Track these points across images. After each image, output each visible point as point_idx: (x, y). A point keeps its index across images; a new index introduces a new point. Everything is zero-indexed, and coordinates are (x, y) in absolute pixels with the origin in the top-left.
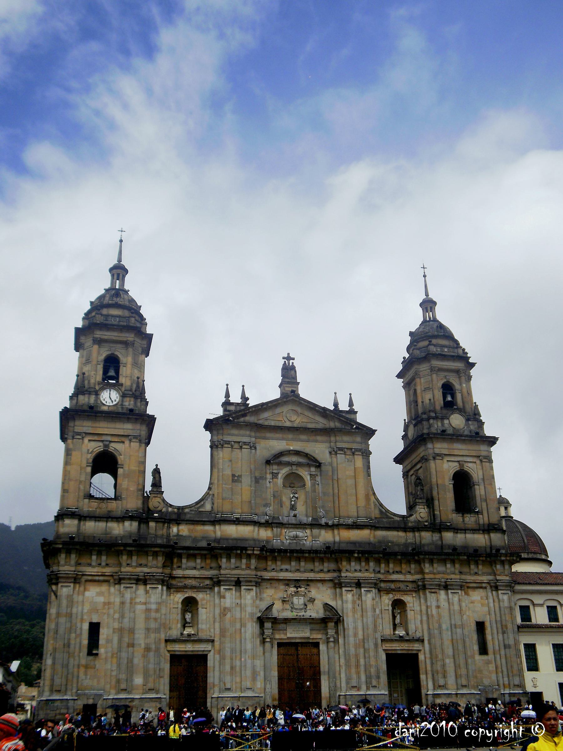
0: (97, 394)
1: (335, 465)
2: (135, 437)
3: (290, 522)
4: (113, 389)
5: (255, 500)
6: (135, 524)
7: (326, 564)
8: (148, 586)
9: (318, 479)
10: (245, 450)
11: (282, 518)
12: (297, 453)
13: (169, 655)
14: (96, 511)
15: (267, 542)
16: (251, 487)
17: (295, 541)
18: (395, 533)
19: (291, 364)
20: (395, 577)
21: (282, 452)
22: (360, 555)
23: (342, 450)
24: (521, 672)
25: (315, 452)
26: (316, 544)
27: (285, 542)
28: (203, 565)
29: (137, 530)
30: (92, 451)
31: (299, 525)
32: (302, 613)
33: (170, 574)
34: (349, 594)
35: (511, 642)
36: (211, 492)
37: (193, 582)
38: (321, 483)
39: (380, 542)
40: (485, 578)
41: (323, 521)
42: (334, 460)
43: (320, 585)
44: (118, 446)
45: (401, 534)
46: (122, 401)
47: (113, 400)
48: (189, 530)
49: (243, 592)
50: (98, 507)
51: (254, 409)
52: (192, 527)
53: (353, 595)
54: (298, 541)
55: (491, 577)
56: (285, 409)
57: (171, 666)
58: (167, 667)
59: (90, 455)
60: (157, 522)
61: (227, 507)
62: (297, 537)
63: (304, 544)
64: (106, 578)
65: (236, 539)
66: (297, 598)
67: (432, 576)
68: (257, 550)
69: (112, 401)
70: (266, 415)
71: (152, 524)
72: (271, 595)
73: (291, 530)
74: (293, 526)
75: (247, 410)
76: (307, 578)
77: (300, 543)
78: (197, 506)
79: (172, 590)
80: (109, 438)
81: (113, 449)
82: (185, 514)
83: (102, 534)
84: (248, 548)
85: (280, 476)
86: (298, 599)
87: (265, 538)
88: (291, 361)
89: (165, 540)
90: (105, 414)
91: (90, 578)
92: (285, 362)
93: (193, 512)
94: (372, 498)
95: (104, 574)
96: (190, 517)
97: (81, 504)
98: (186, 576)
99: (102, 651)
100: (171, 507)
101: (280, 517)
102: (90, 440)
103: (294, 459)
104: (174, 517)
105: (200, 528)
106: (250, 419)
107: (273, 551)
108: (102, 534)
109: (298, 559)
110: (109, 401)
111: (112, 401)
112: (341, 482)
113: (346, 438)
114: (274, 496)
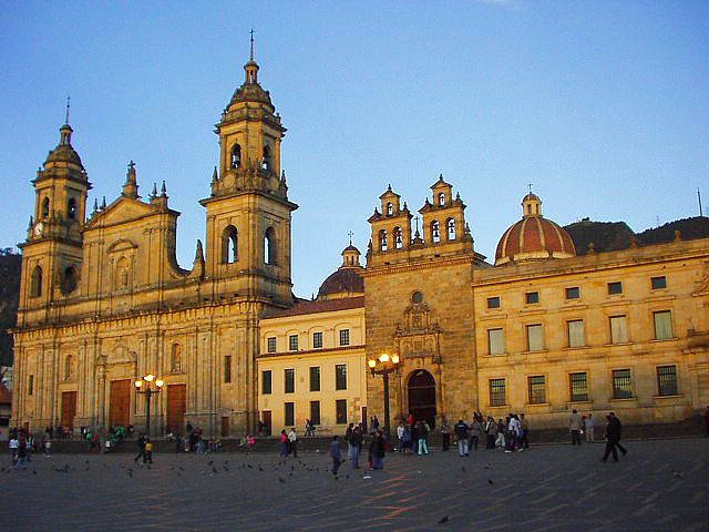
13: (60, 393)
18: (177, 290)
20: (173, 326)
24: (255, 394)
32: (121, 360)
35: (241, 372)
39: (167, 301)
40: (232, 319)
41: (135, 290)
43: (132, 337)
45: (181, 290)
55: (236, 318)
57: (63, 398)
58: (60, 400)
67: (192, 323)
70: (111, 216)
94: (167, 265)
99: (34, 391)
103: (123, 245)
105: (74, 307)
106: (101, 222)
113: (151, 220)
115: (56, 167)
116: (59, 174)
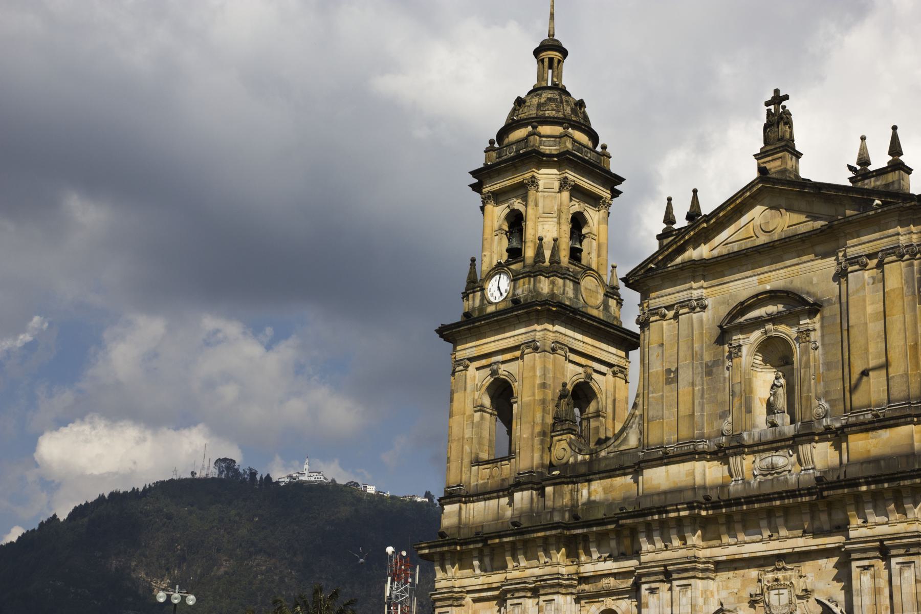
0: (482, 289)
1: (844, 300)
2: (528, 344)
3: (763, 440)
4: (503, 272)
5: (702, 410)
6: (527, 494)
7: (824, 517)
8: (542, 598)
9: (815, 336)
10: (683, 316)
11: (750, 435)
12: (773, 296)
14: (488, 482)
15: (723, 486)
16: (693, 384)
17: (770, 477)
19: (781, 110)
21: (742, 303)
22: (873, 487)
23: (857, 263)
25: (811, 283)
26: (806, 477)
27: (752, 482)
28: (622, 549)
29: (529, 505)
30: (482, 386)
31: (758, 445)
33: (577, 573)
34: (865, 574)
36: (637, 412)
37: (611, 582)
38: (823, 345)
42: (844, 286)
44: (513, 367)
46: (515, 288)
47: (503, 291)
48: (605, 490)
49: (676, 590)
50: (491, 476)
51: (692, 233)
52: (608, 481)
53: (874, 577)
54: (775, 475)
56: (758, 214)
59: (479, 392)
60: (554, 484)
61: (654, 438)
62: (772, 468)
63: (786, 480)
64: (496, 593)
65: (665, 493)
66: (776, 592)
68: (684, 509)
69: (501, 294)
71: (549, 490)
72: (736, 591)
73: (764, 455)
74: (765, 447)
75: (680, 240)
76: (791, 550)
77: (778, 480)
78: (616, 443)
79: (583, 602)
80: (500, 358)
81: (507, 373)
82: (599, 460)
83: (493, 521)
84: (668, 508)
85: (744, 350)
86: (779, 594)
87: (720, 481)
88: (784, 103)
89: (567, 515)
90: (484, 320)
91: (477, 595)
92: (769, 111)
93: (612, 455)
95: (490, 586)
96: (606, 465)
97: (465, 477)
98: (599, 573)
100: (580, 454)
101: (745, 435)
102: (478, 369)
103: (771, 309)
104: (583, 470)
107: (716, 506)
108: (493, 521)
109: (770, 514)
110: (497, 294)
111: (501, 294)
112: (852, 331)
114: (733, 394)
115: (541, 136)
116: (549, 148)
